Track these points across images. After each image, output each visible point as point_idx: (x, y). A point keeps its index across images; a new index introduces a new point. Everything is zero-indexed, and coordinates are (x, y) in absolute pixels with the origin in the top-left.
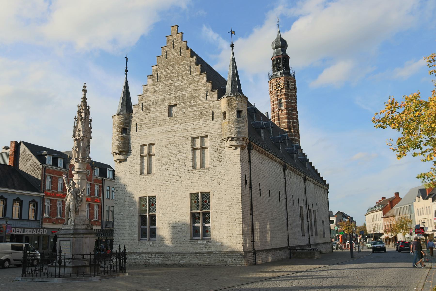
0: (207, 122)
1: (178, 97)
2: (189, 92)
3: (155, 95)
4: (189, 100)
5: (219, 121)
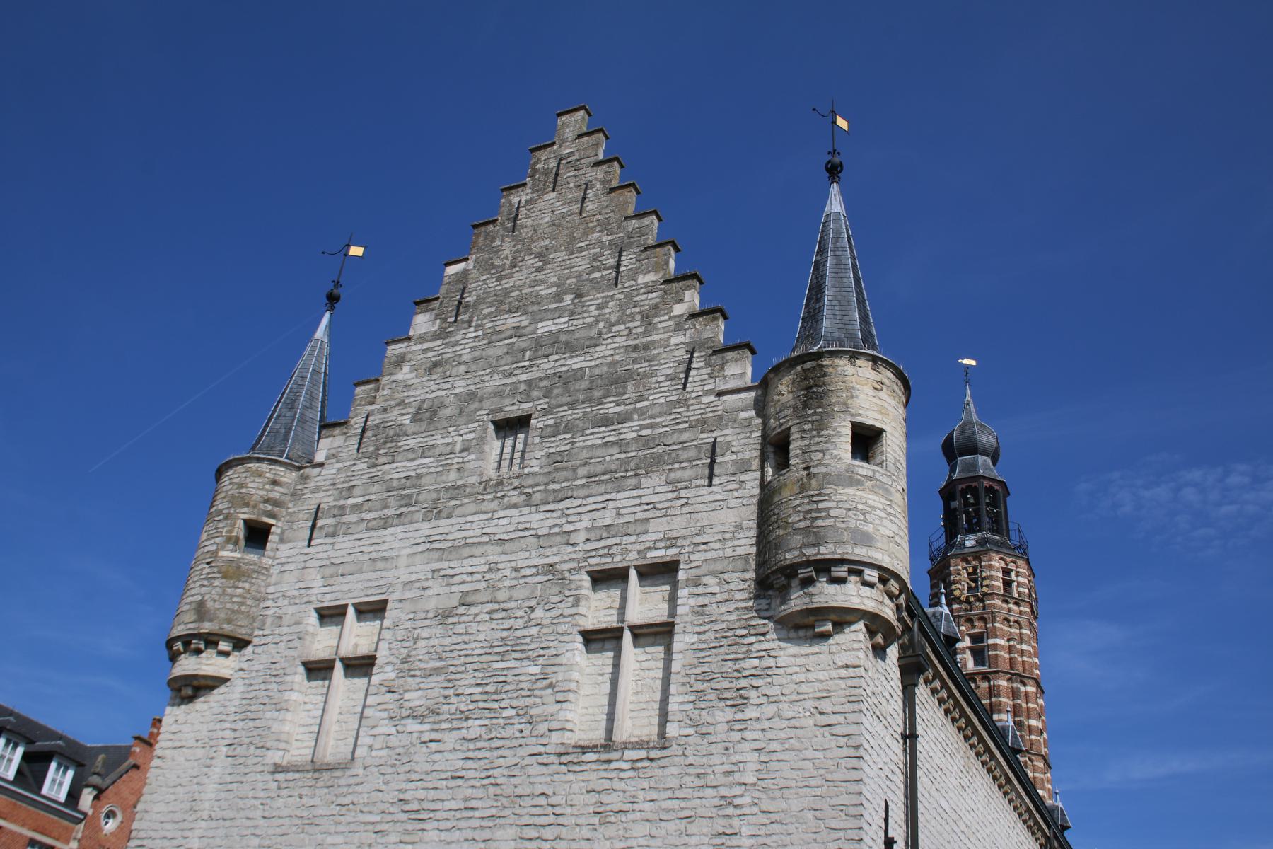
0: (683, 493)
1: (545, 383)
2: (604, 357)
3: (434, 377)
4: (597, 394)
5: (749, 485)
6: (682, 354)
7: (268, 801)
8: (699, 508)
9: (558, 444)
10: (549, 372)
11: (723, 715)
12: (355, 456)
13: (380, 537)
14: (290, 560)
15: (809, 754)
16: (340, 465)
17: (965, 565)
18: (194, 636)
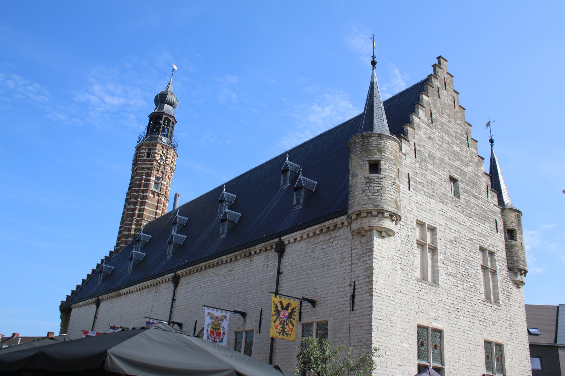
3: (431, 143)
8: (496, 239)
10: (459, 167)
11: (507, 302)
14: (404, 192)
16: (411, 160)
18: (395, 214)
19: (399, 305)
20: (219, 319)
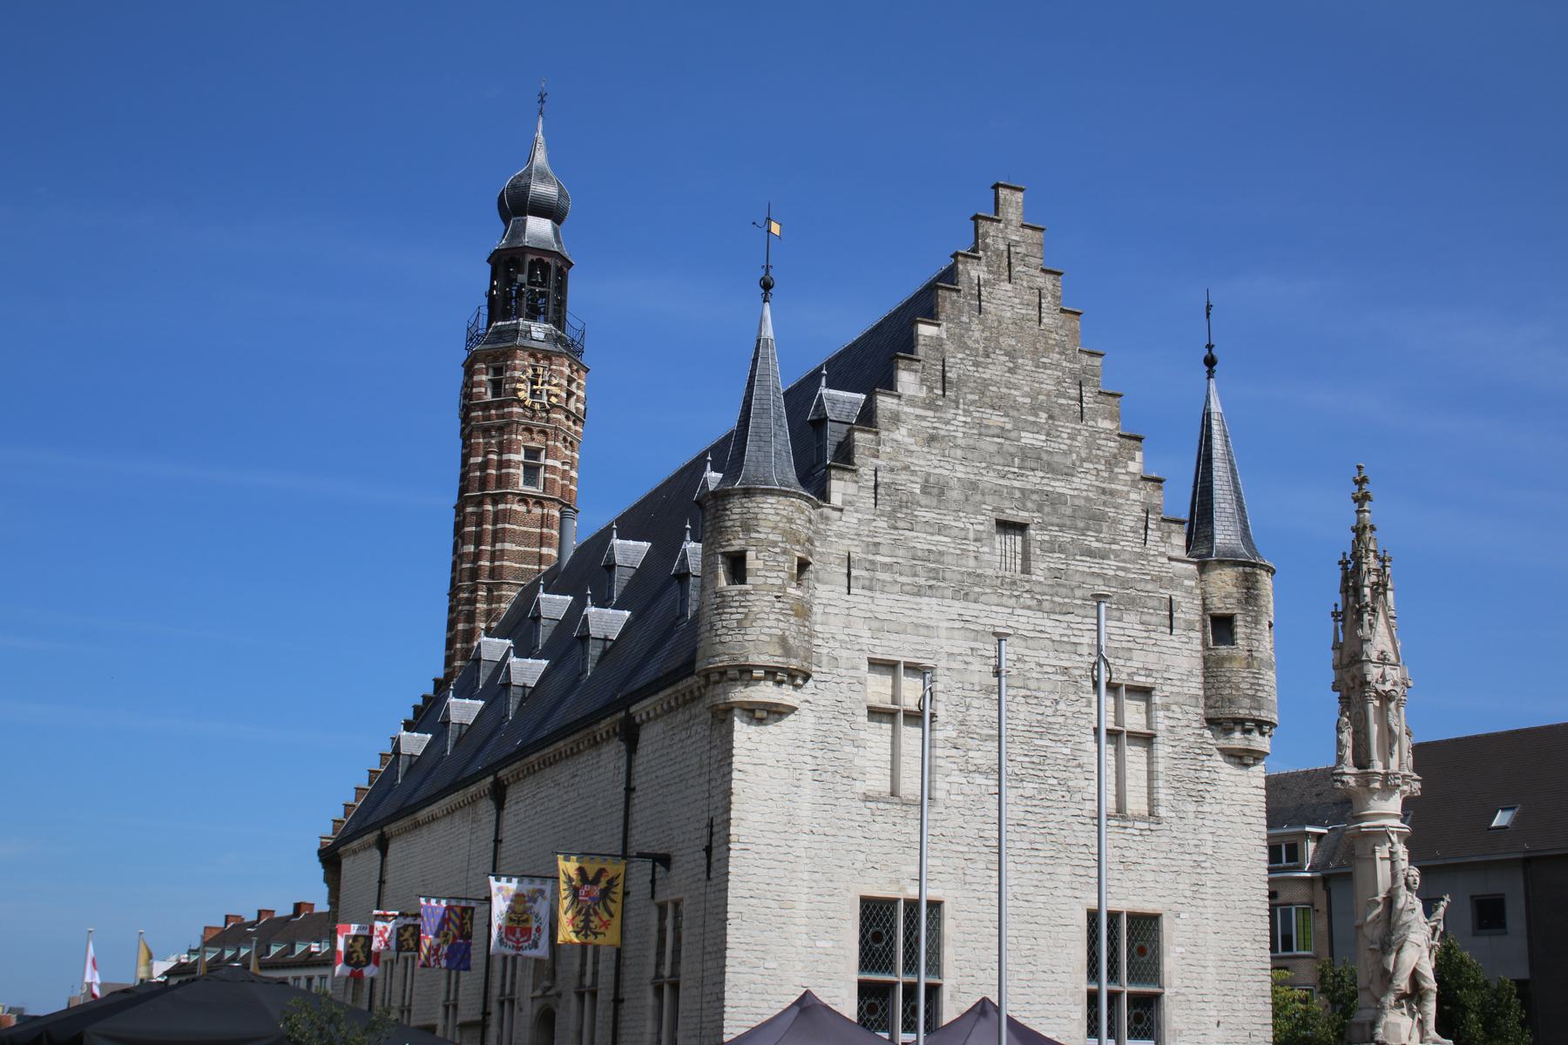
0: (1153, 635)
1: (1035, 497)
3: (934, 451)
4: (1081, 524)
6: (1138, 511)
7: (866, 824)
8: (1165, 650)
9: (1056, 561)
10: (1037, 486)
11: (1191, 807)
12: (873, 511)
13: (917, 604)
15: (1240, 840)
16: (860, 516)
17: (532, 361)
19: (807, 861)
20: (527, 899)
